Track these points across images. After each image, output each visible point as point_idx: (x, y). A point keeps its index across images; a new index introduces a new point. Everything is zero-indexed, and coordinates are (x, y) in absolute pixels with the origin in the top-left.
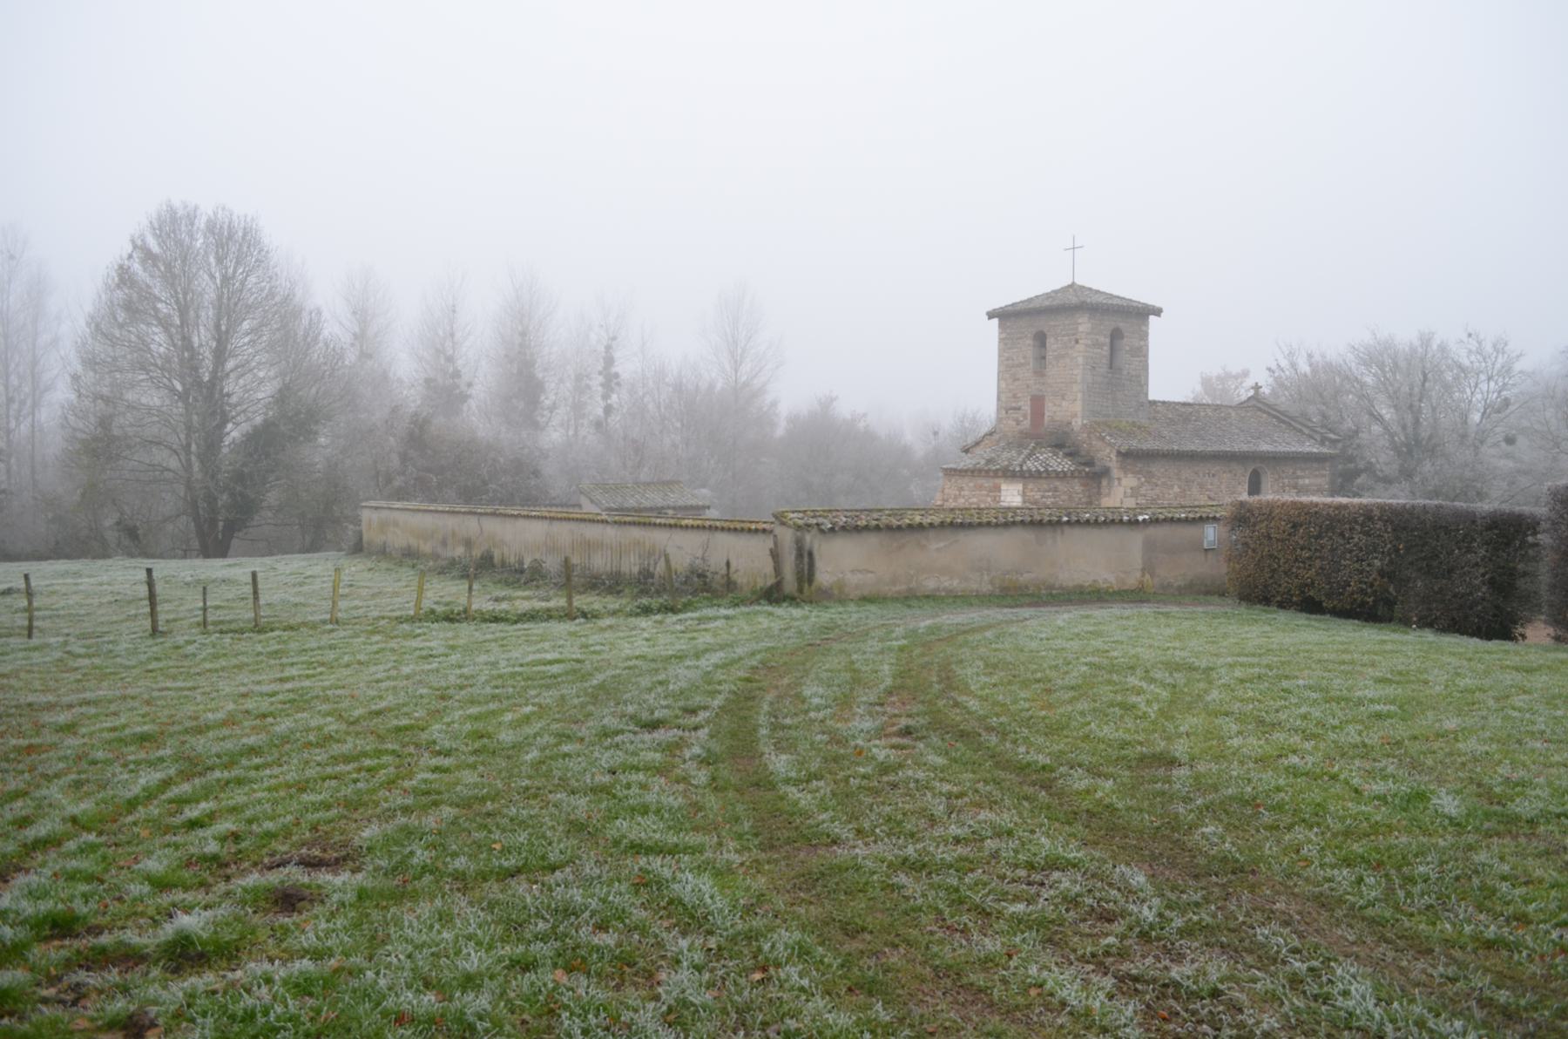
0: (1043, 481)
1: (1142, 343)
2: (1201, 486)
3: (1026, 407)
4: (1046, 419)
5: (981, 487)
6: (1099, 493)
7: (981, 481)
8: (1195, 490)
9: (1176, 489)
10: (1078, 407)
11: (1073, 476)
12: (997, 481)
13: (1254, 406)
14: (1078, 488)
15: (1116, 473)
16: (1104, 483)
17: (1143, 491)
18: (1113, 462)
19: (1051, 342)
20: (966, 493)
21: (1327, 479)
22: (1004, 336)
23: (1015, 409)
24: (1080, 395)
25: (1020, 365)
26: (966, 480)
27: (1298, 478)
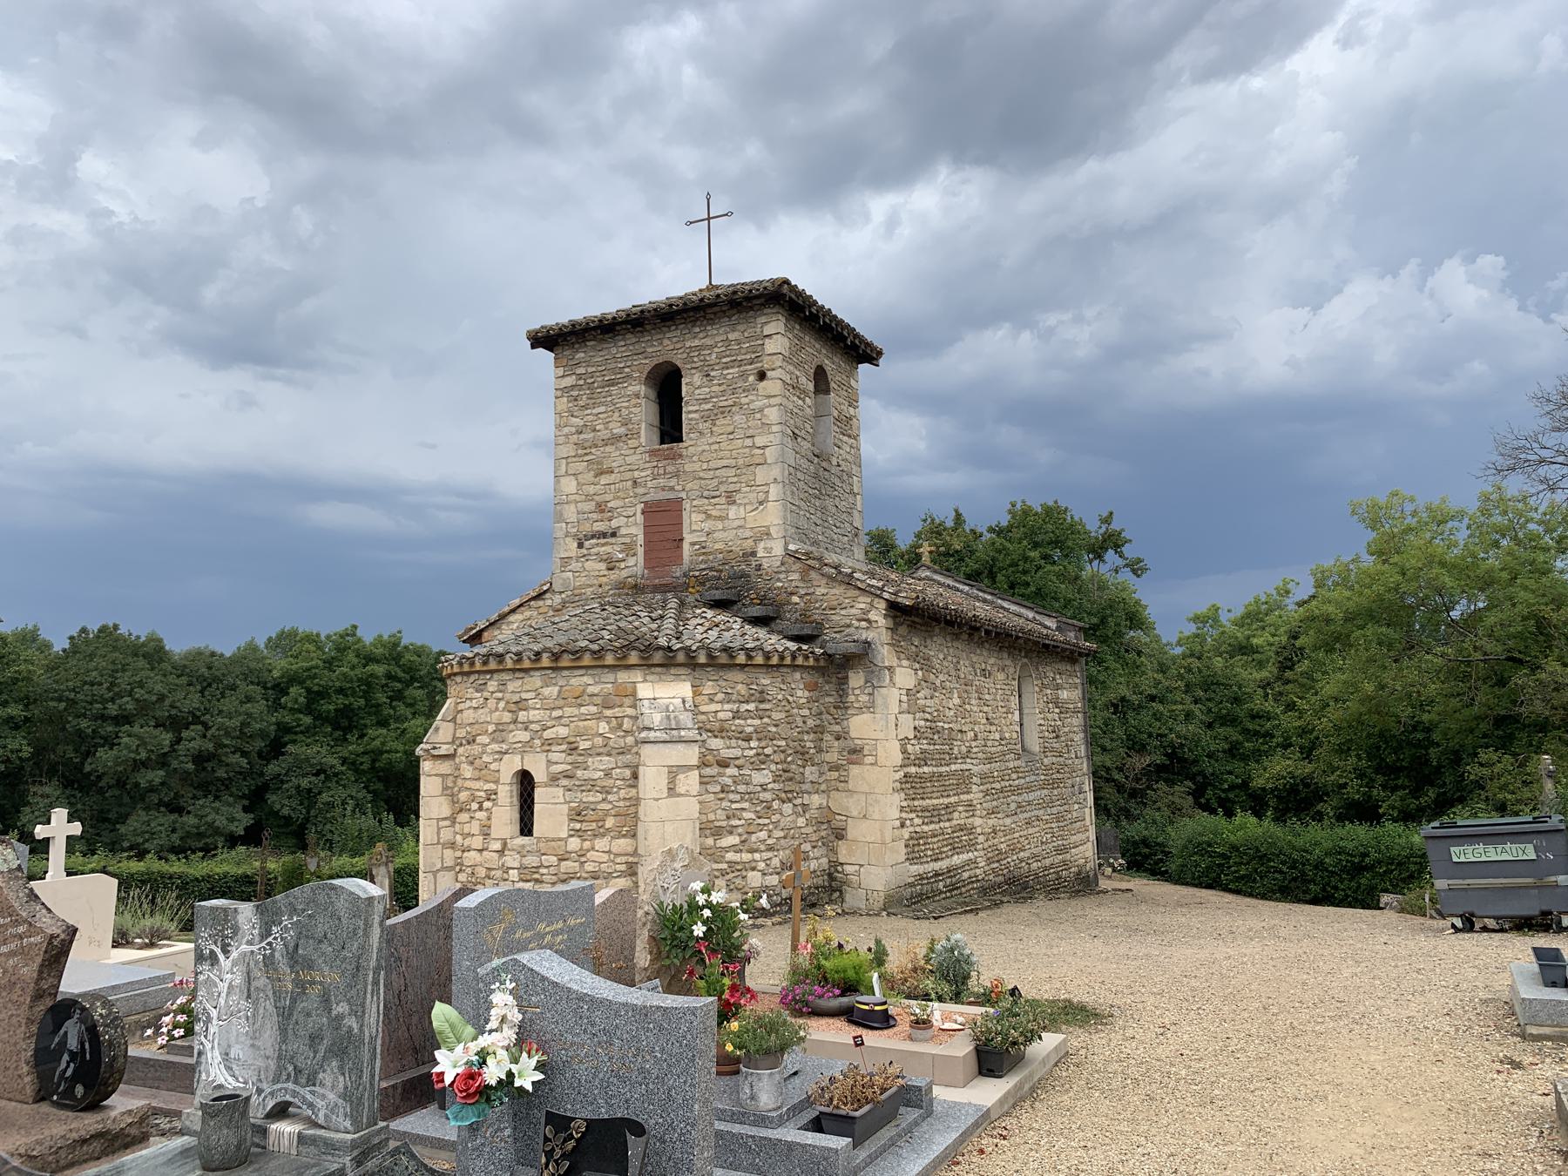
0: (738, 676)
3: (634, 529)
4: (686, 546)
5: (579, 698)
6: (842, 705)
7: (579, 681)
10: (773, 516)
11: (794, 667)
12: (623, 676)
13: (927, 578)
14: (802, 694)
15: (885, 654)
16: (856, 679)
18: (878, 628)
19: (691, 386)
20: (534, 715)
22: (569, 381)
23: (604, 535)
24: (775, 491)
25: (615, 439)
26: (535, 680)
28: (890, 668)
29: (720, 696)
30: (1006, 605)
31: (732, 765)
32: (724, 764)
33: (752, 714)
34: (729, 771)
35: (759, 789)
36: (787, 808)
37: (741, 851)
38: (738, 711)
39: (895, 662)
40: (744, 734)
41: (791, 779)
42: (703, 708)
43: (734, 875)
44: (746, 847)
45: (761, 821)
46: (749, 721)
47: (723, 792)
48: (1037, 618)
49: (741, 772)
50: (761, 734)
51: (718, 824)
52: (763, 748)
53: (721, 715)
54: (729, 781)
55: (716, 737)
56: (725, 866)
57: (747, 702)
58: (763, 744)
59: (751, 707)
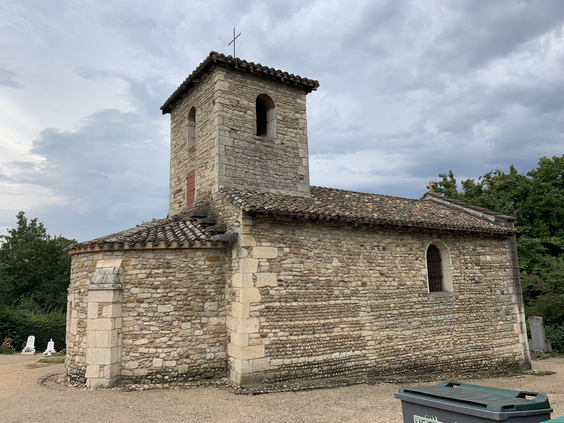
0: (151, 255)
1: (298, 116)
2: (370, 261)
8: (362, 264)
9: (336, 263)
11: (191, 247)
13: (430, 200)
15: (243, 240)
17: (287, 263)
21: (508, 256)
27: (479, 254)
28: (247, 248)
29: (139, 266)
30: (468, 210)
31: (145, 302)
32: (140, 301)
33: (159, 275)
34: (142, 305)
35: (163, 314)
36: (187, 325)
37: (149, 347)
38: (151, 274)
39: (253, 243)
40: (153, 286)
41: (190, 309)
42: (129, 273)
43: (143, 359)
44: (153, 345)
45: (163, 332)
46: (157, 279)
47: (139, 316)
48: (485, 216)
49: (150, 306)
50: (167, 286)
51: (134, 332)
52: (167, 293)
53: (139, 276)
54: (142, 310)
55: (137, 287)
56: (138, 355)
57: (158, 269)
58: (167, 291)
59: (160, 271)
